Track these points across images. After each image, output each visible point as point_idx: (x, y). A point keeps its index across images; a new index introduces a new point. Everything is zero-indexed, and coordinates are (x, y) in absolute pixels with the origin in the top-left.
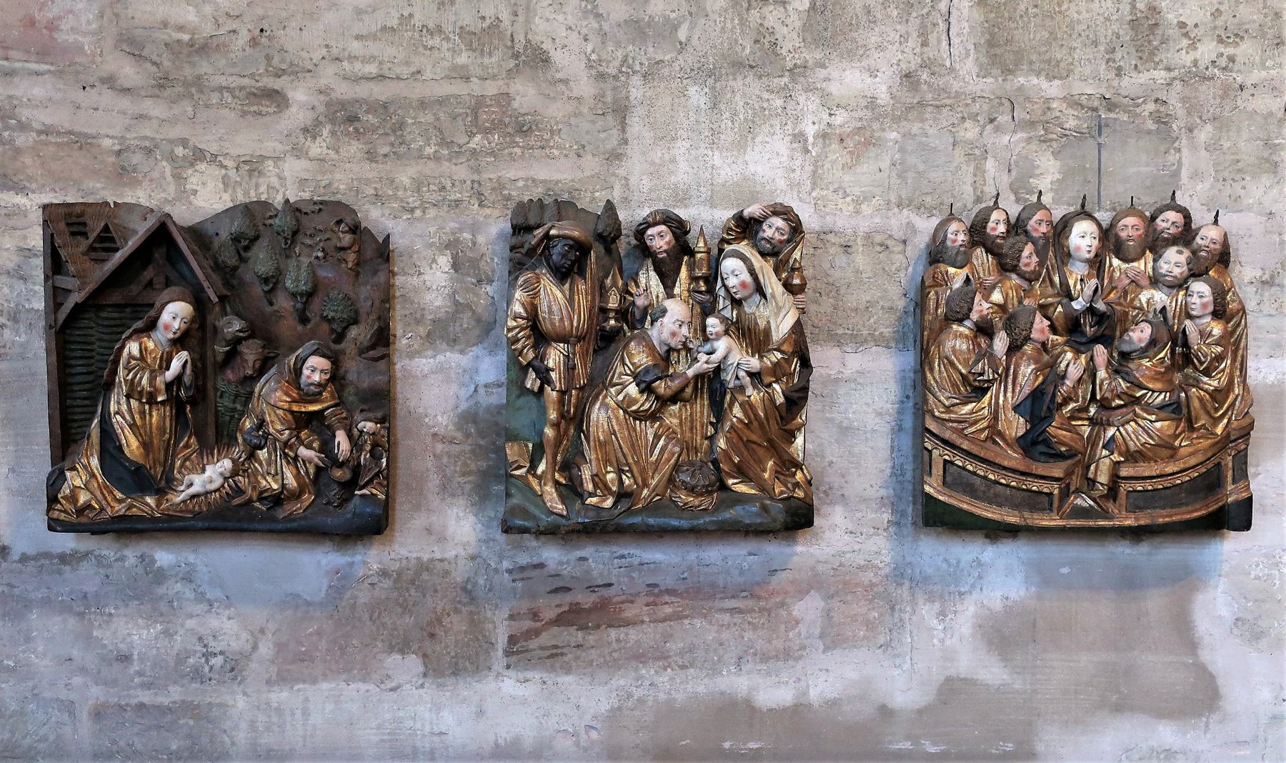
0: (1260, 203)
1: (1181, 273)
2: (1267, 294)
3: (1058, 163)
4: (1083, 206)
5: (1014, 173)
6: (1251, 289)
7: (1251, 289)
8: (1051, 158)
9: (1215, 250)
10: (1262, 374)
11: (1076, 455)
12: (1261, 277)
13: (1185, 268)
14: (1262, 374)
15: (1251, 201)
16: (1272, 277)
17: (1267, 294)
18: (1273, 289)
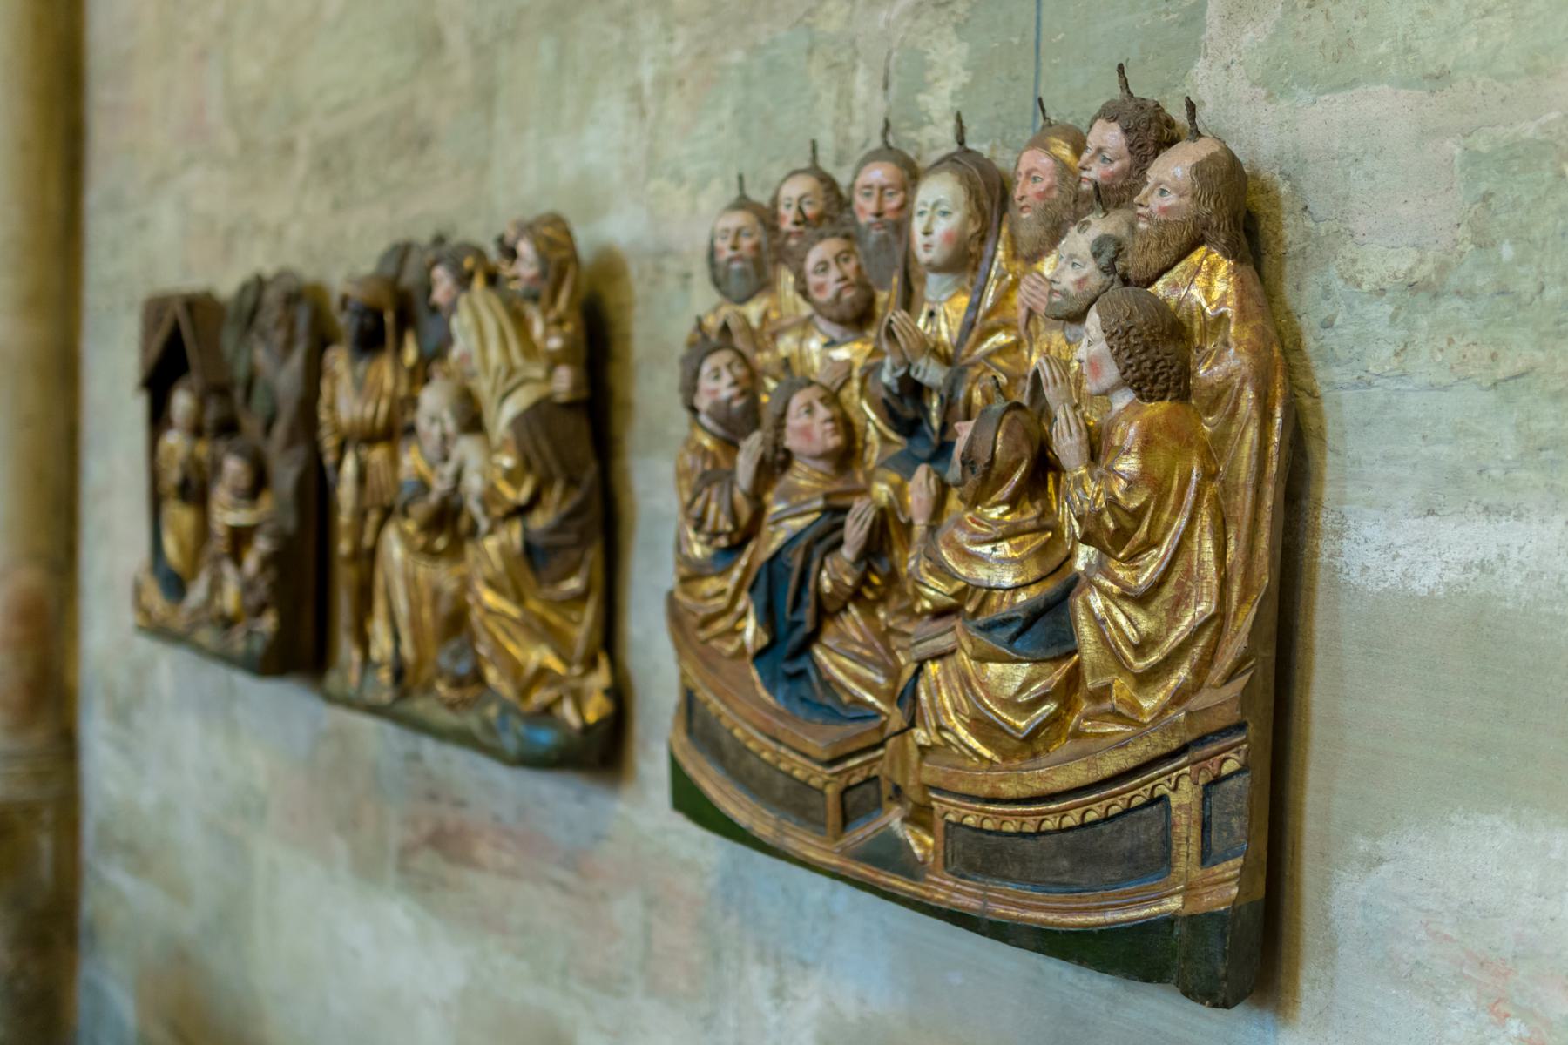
0: (1409, 50)
1: (1080, 282)
2: (1423, 322)
3: (963, 49)
4: (961, 142)
5: (893, 89)
6: (1380, 311)
7: (1380, 311)
8: (954, 39)
9: (1164, 210)
10: (1400, 565)
11: (875, 717)
12: (1411, 271)
13: (1090, 267)
14: (1400, 565)
15: (1383, 48)
16: (1443, 268)
17: (1423, 322)
18: (1447, 306)
